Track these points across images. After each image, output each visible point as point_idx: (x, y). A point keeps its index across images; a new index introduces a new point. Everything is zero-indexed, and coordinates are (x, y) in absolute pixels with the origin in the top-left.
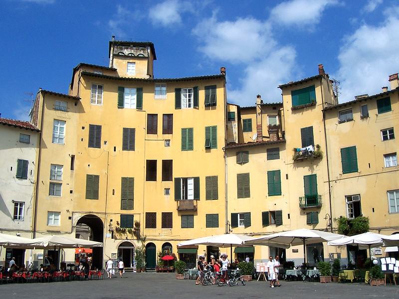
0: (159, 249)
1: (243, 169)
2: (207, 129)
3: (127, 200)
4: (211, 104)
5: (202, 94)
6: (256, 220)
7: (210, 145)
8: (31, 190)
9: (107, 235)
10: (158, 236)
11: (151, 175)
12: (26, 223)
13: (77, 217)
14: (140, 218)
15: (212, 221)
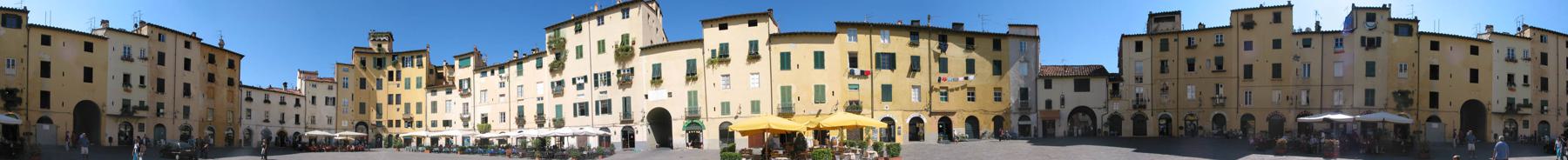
0: (394, 135)
1: (434, 98)
2: (417, 78)
3: (379, 114)
4: (420, 65)
5: (415, 60)
6: (440, 124)
7: (419, 86)
8: (335, 111)
9: (370, 131)
10: (394, 130)
11: (390, 102)
12: (333, 126)
13: (356, 123)
14: (385, 124)
15: (420, 125)
